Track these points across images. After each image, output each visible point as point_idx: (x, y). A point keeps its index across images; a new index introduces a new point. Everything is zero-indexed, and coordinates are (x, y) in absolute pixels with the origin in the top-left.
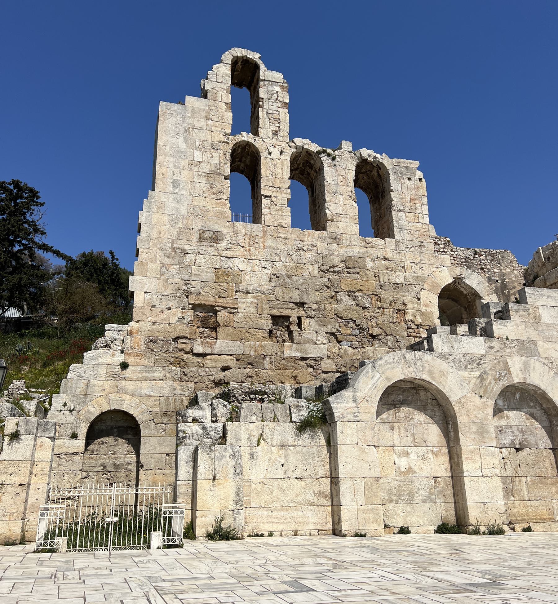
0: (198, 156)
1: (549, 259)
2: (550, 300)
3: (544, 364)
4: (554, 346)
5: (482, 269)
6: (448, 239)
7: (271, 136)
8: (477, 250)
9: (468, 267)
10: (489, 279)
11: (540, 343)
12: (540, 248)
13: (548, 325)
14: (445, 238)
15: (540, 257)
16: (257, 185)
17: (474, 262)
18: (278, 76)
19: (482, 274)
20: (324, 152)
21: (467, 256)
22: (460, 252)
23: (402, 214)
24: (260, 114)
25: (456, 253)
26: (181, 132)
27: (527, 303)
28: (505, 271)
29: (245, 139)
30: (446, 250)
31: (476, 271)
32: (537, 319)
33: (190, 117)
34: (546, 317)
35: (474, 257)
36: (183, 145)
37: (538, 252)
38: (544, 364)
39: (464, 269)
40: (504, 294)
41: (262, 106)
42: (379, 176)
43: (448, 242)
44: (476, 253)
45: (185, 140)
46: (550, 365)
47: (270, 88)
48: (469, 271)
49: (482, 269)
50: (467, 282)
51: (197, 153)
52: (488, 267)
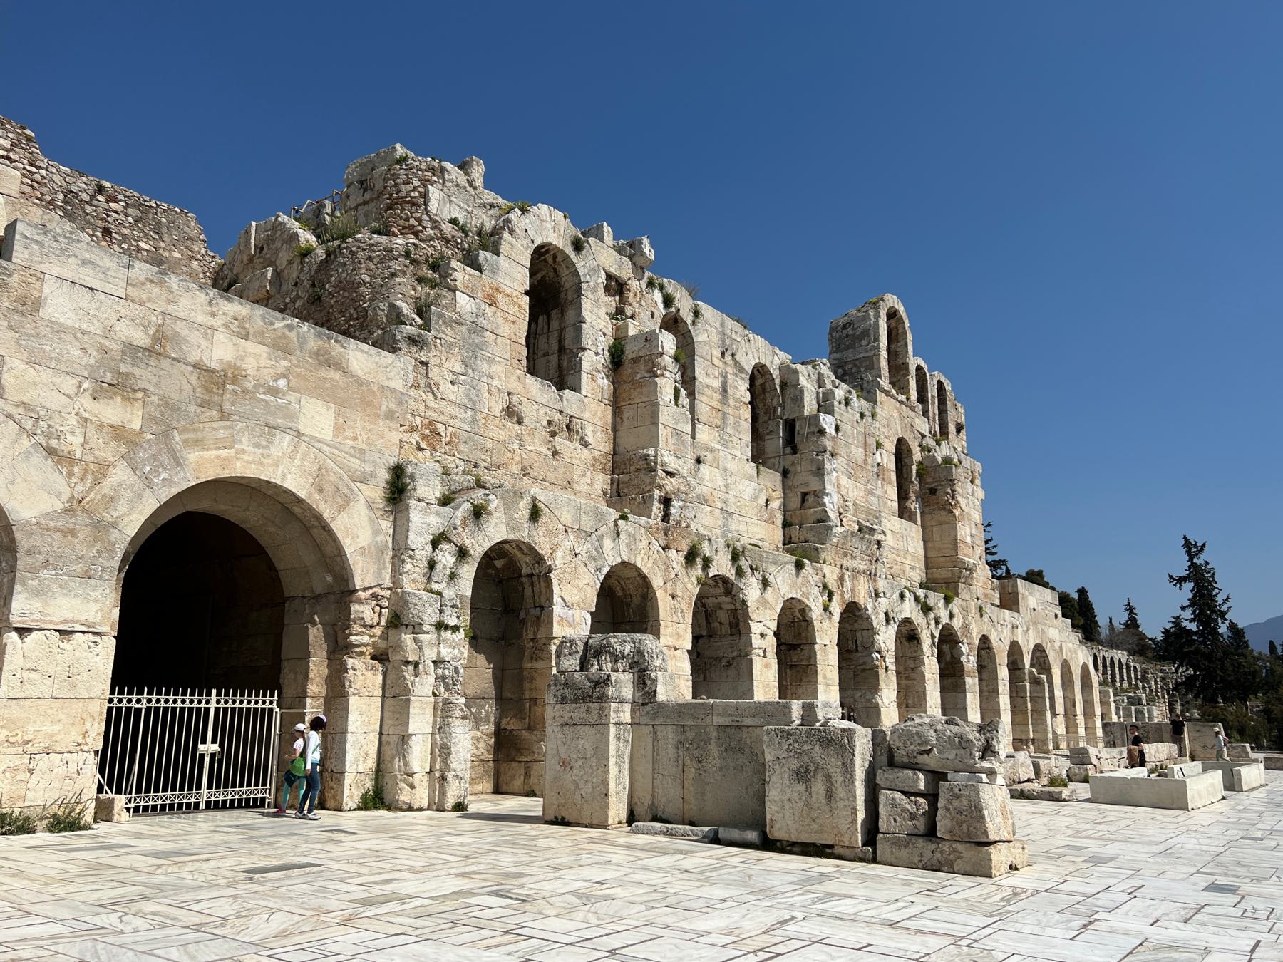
1: (262, 248)
2: (88, 270)
3: (9, 416)
4: (57, 380)
5: (107, 232)
6: (28, 132)
8: (108, 185)
9: (68, 216)
12: (254, 224)
13: (59, 329)
14: (22, 128)
15: (248, 242)
17: (89, 209)
19: (104, 243)
21: (74, 188)
22: (58, 174)
25: (43, 172)
27: (10, 260)
28: (166, 254)
30: (11, 155)
31: (90, 231)
34: (59, 305)
35: (93, 198)
37: (248, 232)
38: (9, 416)
39: (56, 216)
43: (29, 139)
44: (100, 189)
46: (28, 424)
48: (68, 225)
49: (107, 232)
52: (125, 231)
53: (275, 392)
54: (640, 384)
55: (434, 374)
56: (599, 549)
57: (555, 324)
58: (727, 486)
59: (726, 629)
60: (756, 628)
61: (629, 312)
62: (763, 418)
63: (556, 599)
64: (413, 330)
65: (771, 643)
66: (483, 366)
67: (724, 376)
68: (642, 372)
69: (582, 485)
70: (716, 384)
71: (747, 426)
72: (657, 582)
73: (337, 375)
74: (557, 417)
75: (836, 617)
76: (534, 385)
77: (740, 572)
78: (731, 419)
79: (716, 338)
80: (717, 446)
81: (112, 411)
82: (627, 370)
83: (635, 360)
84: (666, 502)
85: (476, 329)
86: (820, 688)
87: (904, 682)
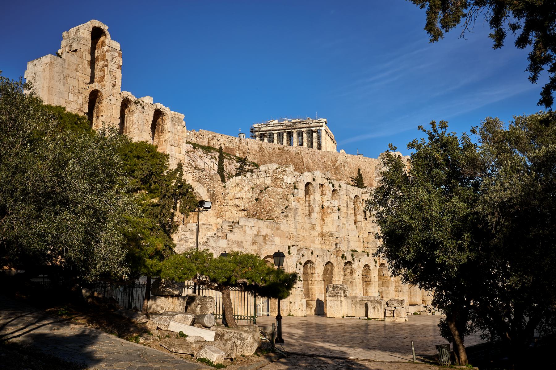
0: (71, 97)
7: (111, 88)
9: (200, 183)
10: (208, 190)
11: (244, 242)
16: (98, 117)
18: (116, 45)
20: (139, 102)
23: (173, 147)
24: (106, 71)
26: (62, 79)
29: (97, 88)
32: (245, 232)
33: (67, 69)
36: (63, 88)
40: (213, 199)
41: (107, 66)
42: (163, 120)
45: (64, 85)
47: (112, 53)
50: (198, 191)
51: (71, 95)
53: (272, 237)
54: (329, 214)
55: (289, 222)
56: (324, 259)
57: (307, 199)
58: (348, 233)
59: (349, 274)
60: (357, 274)
61: (324, 193)
62: (357, 209)
63: (316, 273)
64: (285, 214)
65: (361, 277)
66: (297, 218)
67: (347, 203)
68: (329, 211)
69: (316, 242)
70: (345, 205)
71: (353, 215)
72: (335, 265)
73: (279, 231)
74: (311, 225)
75: (378, 268)
76: (306, 218)
77: (353, 260)
78: (349, 214)
79: (345, 191)
80: (346, 223)
81: (255, 247)
82: (326, 210)
83: (328, 207)
84: (336, 244)
85: (296, 209)
86: (373, 288)
87: (397, 284)
